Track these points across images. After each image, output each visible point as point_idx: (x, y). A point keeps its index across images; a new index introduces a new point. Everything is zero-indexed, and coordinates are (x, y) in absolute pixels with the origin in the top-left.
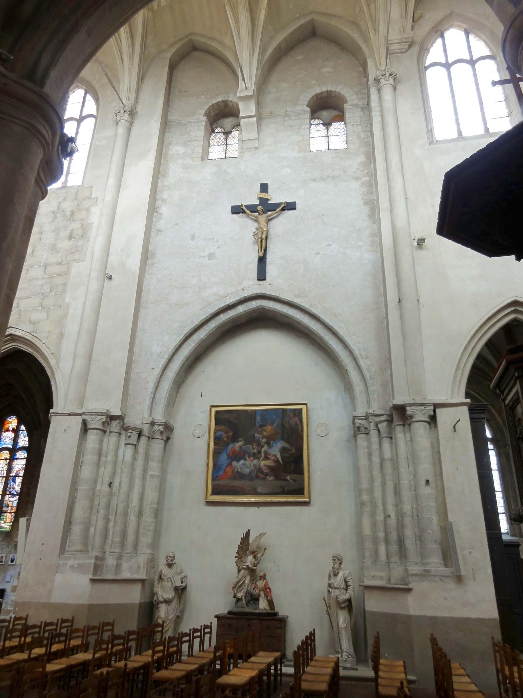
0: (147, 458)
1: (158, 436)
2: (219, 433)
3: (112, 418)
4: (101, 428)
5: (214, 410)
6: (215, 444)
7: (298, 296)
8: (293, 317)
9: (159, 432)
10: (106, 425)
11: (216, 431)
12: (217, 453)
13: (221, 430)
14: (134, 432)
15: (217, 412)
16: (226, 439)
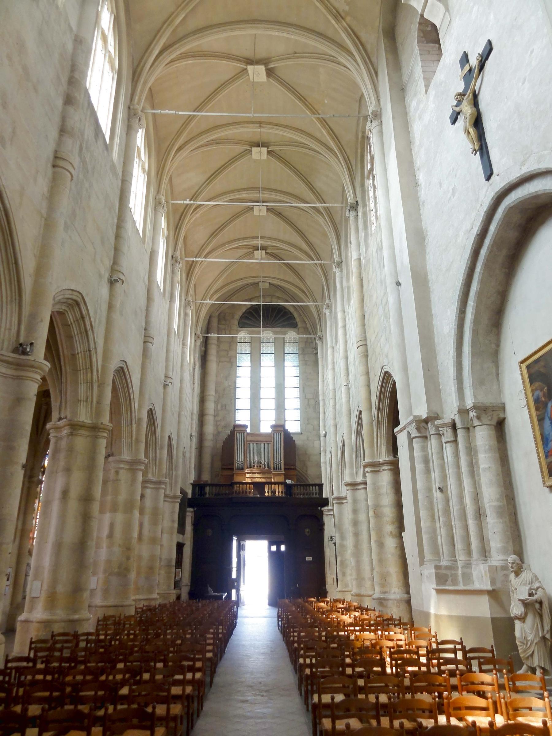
0: (471, 451)
1: (476, 422)
2: (537, 393)
3: (426, 421)
4: (419, 435)
5: (524, 366)
6: (537, 409)
7: (523, 163)
8: (537, 192)
9: (475, 418)
10: (423, 430)
11: (533, 391)
12: (541, 420)
13: (536, 390)
14: (445, 429)
15: (528, 367)
16: (543, 399)
